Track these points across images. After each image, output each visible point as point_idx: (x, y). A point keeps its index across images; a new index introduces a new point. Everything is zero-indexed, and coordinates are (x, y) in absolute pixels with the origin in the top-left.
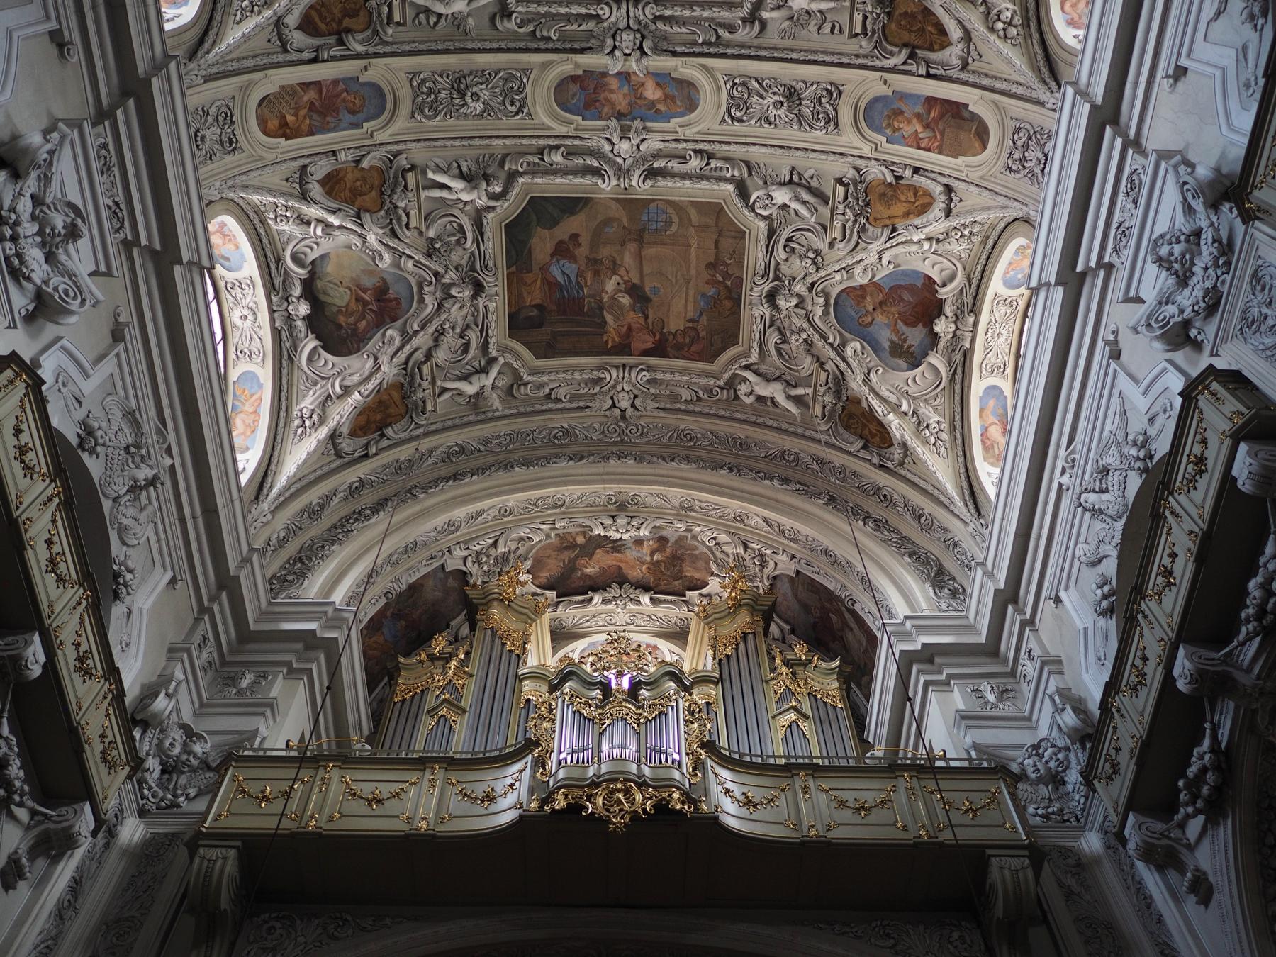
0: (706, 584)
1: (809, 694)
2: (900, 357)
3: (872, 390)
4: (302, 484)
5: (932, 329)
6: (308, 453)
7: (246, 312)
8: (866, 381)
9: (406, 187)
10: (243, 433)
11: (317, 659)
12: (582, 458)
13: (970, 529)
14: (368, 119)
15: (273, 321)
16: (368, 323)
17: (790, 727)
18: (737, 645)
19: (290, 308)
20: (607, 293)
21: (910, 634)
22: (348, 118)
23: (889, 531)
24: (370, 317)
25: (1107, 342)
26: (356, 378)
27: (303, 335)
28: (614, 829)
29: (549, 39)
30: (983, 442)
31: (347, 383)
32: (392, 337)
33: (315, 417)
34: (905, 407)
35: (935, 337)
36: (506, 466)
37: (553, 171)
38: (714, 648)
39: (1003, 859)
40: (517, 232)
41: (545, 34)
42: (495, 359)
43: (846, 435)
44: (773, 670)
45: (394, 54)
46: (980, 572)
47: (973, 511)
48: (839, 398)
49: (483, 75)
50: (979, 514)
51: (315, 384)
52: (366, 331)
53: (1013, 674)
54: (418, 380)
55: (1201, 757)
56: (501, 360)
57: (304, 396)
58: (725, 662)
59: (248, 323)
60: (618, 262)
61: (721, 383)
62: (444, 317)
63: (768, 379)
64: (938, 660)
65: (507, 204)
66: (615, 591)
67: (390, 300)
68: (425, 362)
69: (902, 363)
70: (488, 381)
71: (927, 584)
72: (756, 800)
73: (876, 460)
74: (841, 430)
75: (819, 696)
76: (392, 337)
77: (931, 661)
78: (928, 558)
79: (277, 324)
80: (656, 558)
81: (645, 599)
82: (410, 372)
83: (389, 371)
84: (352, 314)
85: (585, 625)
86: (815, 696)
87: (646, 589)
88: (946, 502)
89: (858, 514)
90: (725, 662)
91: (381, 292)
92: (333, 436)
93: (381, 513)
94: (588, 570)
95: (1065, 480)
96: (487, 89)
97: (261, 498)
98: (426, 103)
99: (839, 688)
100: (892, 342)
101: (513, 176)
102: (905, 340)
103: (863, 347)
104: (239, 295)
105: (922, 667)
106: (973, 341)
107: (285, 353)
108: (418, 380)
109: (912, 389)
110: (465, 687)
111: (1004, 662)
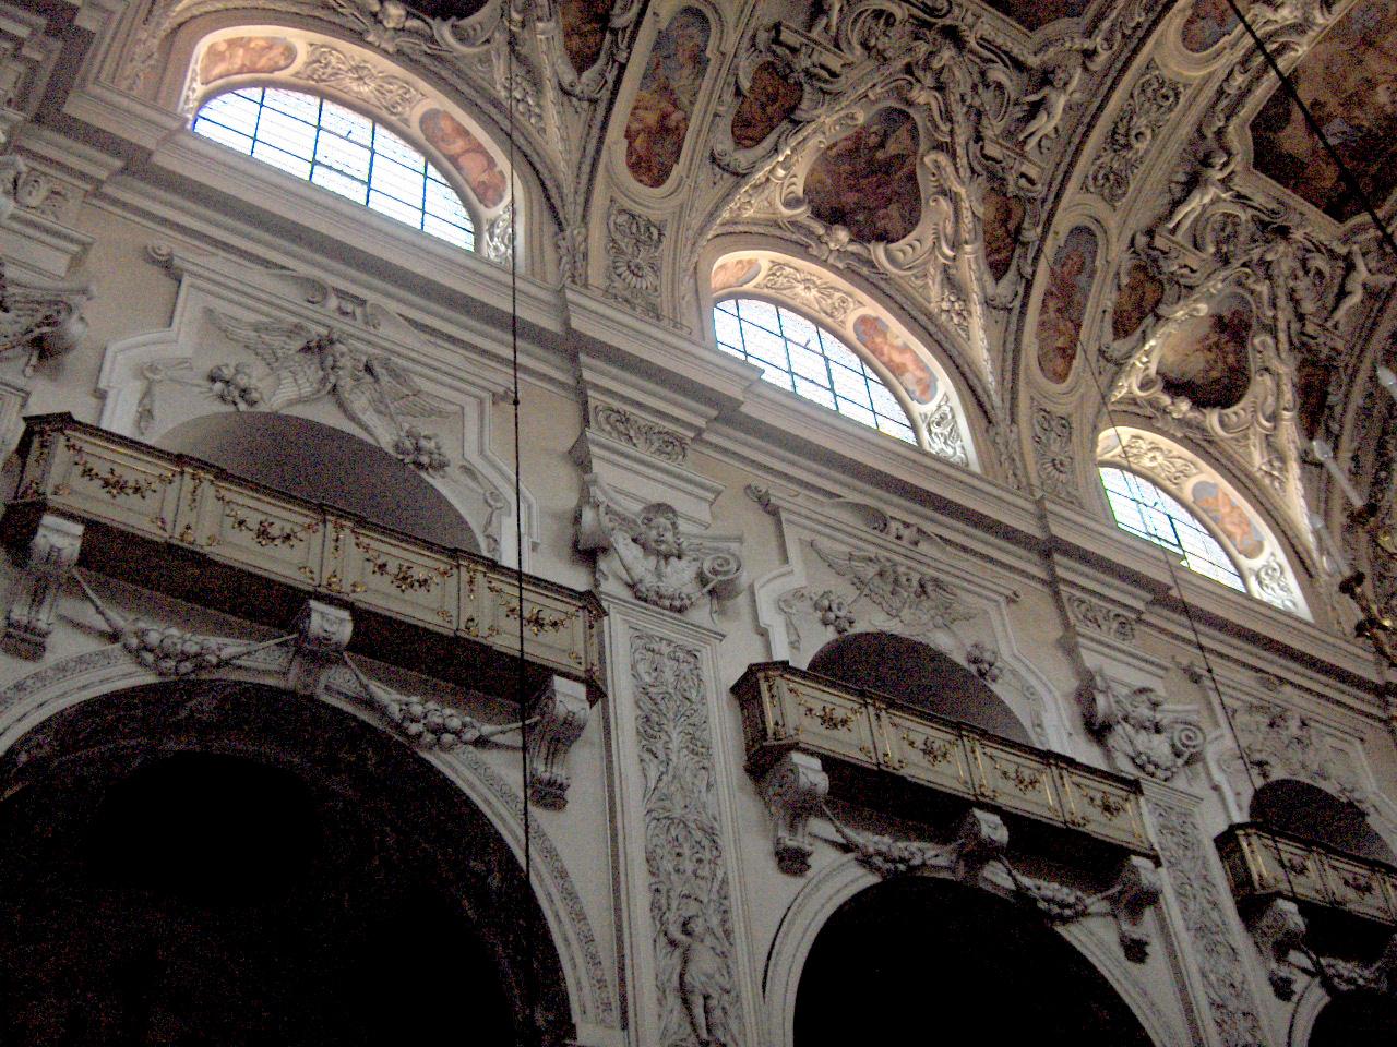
7: (1151, 454)
9: (1163, 252)
10: (1244, 533)
14: (1094, 254)
15: (1173, 437)
19: (1175, 415)
20: (1385, 105)
22: (1082, 279)
24: (1231, 347)
26: (1271, 400)
29: (1139, 25)
31: (1269, 411)
32: (1263, 343)
37: (1244, 94)
40: (1268, 160)
41: (1133, 24)
42: (1350, 253)
45: (1058, 197)
49: (1127, 116)
51: (1246, 437)
54: (1312, 342)
56: (1355, 248)
57: (1250, 454)
59: (1160, 459)
60: (1370, 77)
62: (1281, 281)
65: (1238, 158)
67: (1231, 320)
68: (1304, 325)
70: (1361, 273)
76: (1263, 343)
79: (1179, 435)
82: (1302, 346)
91: (1220, 323)
96: (1140, 117)
98: (1113, 184)
101: (1220, 133)
104: (1135, 451)
107: (1205, 444)
108: (1312, 342)
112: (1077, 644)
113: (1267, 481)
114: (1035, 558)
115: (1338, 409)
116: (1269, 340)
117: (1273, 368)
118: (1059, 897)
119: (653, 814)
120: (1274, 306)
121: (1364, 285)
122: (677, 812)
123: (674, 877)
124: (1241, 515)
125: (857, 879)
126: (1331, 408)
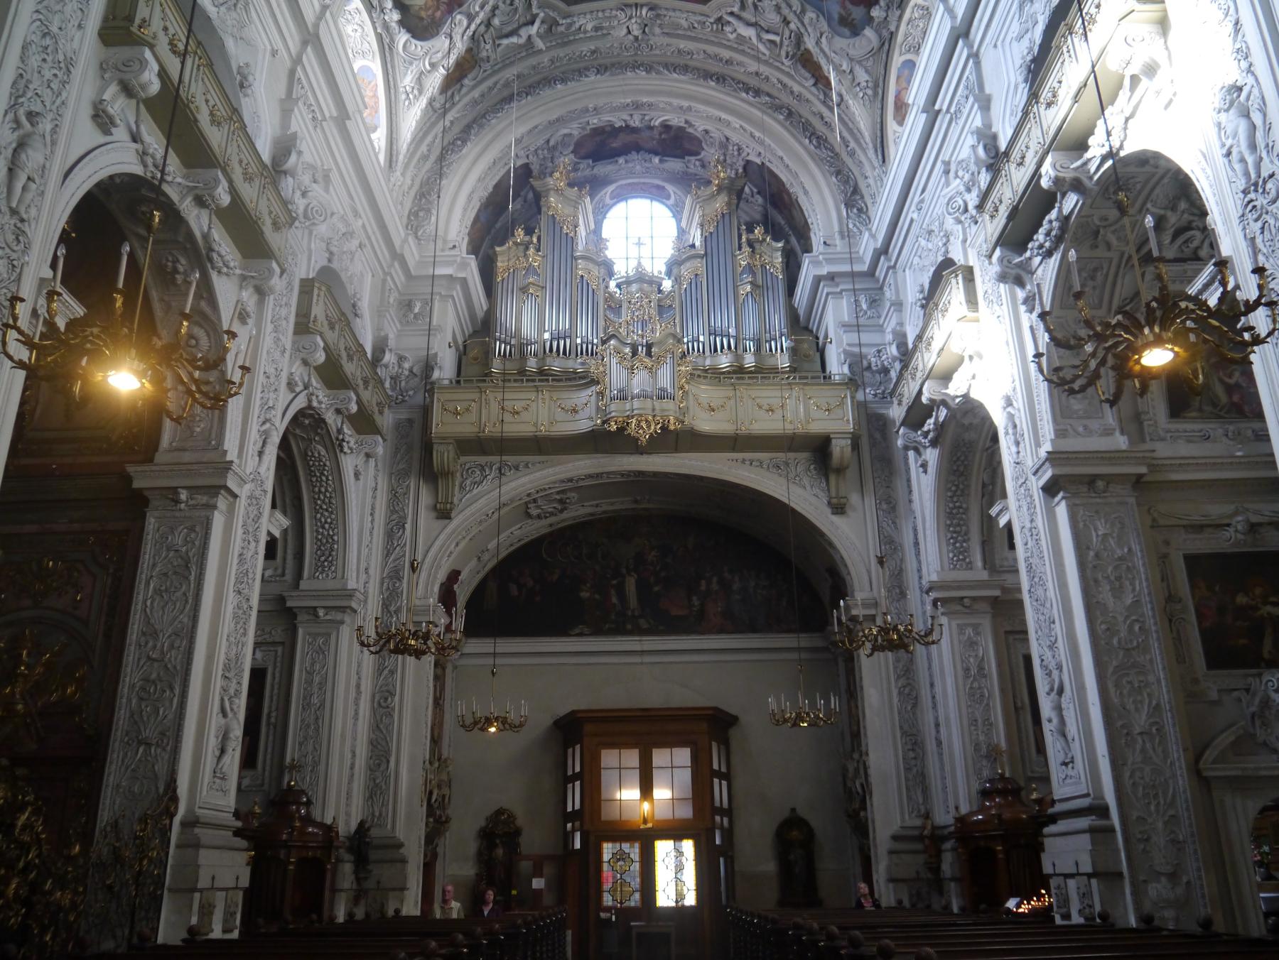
0: (699, 154)
1: (762, 266)
2: (845, 26)
3: (822, 50)
4: (418, 139)
5: (869, 12)
7: (356, 27)
8: (818, 43)
12: (606, 69)
13: (875, 174)
15: (375, 29)
16: (442, 12)
19: (386, 18)
21: (821, 262)
23: (826, 148)
24: (443, 7)
25: (943, 162)
26: (440, 55)
27: (397, 31)
30: (896, 104)
31: (434, 60)
32: (460, 20)
33: (416, 92)
34: (844, 67)
35: (871, 19)
36: (550, 82)
38: (702, 226)
42: (537, 14)
43: (802, 71)
44: (740, 248)
46: (867, 235)
47: (880, 157)
48: (799, 49)
50: (884, 161)
51: (411, 64)
52: (441, 19)
53: (881, 288)
55: (1050, 222)
57: (405, 74)
58: (709, 239)
59: (358, 34)
61: (712, 20)
63: (749, 24)
64: (837, 280)
66: (634, 155)
69: (846, 31)
70: (533, 30)
71: (843, 206)
73: (822, 97)
74: (800, 67)
79: (379, 31)
81: (656, 160)
83: (460, 46)
84: (429, 9)
87: (656, 154)
88: (864, 145)
89: (807, 130)
90: (709, 239)
92: (431, 102)
93: (469, 143)
94: (614, 145)
95: (915, 216)
97: (394, 165)
100: (841, 15)
102: (850, 14)
103: (818, 16)
104: (350, 17)
106: (898, 27)
107: (387, 47)
109: (852, 52)
111: (878, 281)
112: (293, 110)
113: (404, 97)
114: (297, 38)
115: (464, 90)
116: (465, 23)
117: (454, 39)
118: (228, 258)
119: (41, 17)
120: (482, 7)
121: (530, 37)
122: (54, 29)
123: (36, 74)
124: (377, 103)
125: (130, 163)
126: (462, 85)
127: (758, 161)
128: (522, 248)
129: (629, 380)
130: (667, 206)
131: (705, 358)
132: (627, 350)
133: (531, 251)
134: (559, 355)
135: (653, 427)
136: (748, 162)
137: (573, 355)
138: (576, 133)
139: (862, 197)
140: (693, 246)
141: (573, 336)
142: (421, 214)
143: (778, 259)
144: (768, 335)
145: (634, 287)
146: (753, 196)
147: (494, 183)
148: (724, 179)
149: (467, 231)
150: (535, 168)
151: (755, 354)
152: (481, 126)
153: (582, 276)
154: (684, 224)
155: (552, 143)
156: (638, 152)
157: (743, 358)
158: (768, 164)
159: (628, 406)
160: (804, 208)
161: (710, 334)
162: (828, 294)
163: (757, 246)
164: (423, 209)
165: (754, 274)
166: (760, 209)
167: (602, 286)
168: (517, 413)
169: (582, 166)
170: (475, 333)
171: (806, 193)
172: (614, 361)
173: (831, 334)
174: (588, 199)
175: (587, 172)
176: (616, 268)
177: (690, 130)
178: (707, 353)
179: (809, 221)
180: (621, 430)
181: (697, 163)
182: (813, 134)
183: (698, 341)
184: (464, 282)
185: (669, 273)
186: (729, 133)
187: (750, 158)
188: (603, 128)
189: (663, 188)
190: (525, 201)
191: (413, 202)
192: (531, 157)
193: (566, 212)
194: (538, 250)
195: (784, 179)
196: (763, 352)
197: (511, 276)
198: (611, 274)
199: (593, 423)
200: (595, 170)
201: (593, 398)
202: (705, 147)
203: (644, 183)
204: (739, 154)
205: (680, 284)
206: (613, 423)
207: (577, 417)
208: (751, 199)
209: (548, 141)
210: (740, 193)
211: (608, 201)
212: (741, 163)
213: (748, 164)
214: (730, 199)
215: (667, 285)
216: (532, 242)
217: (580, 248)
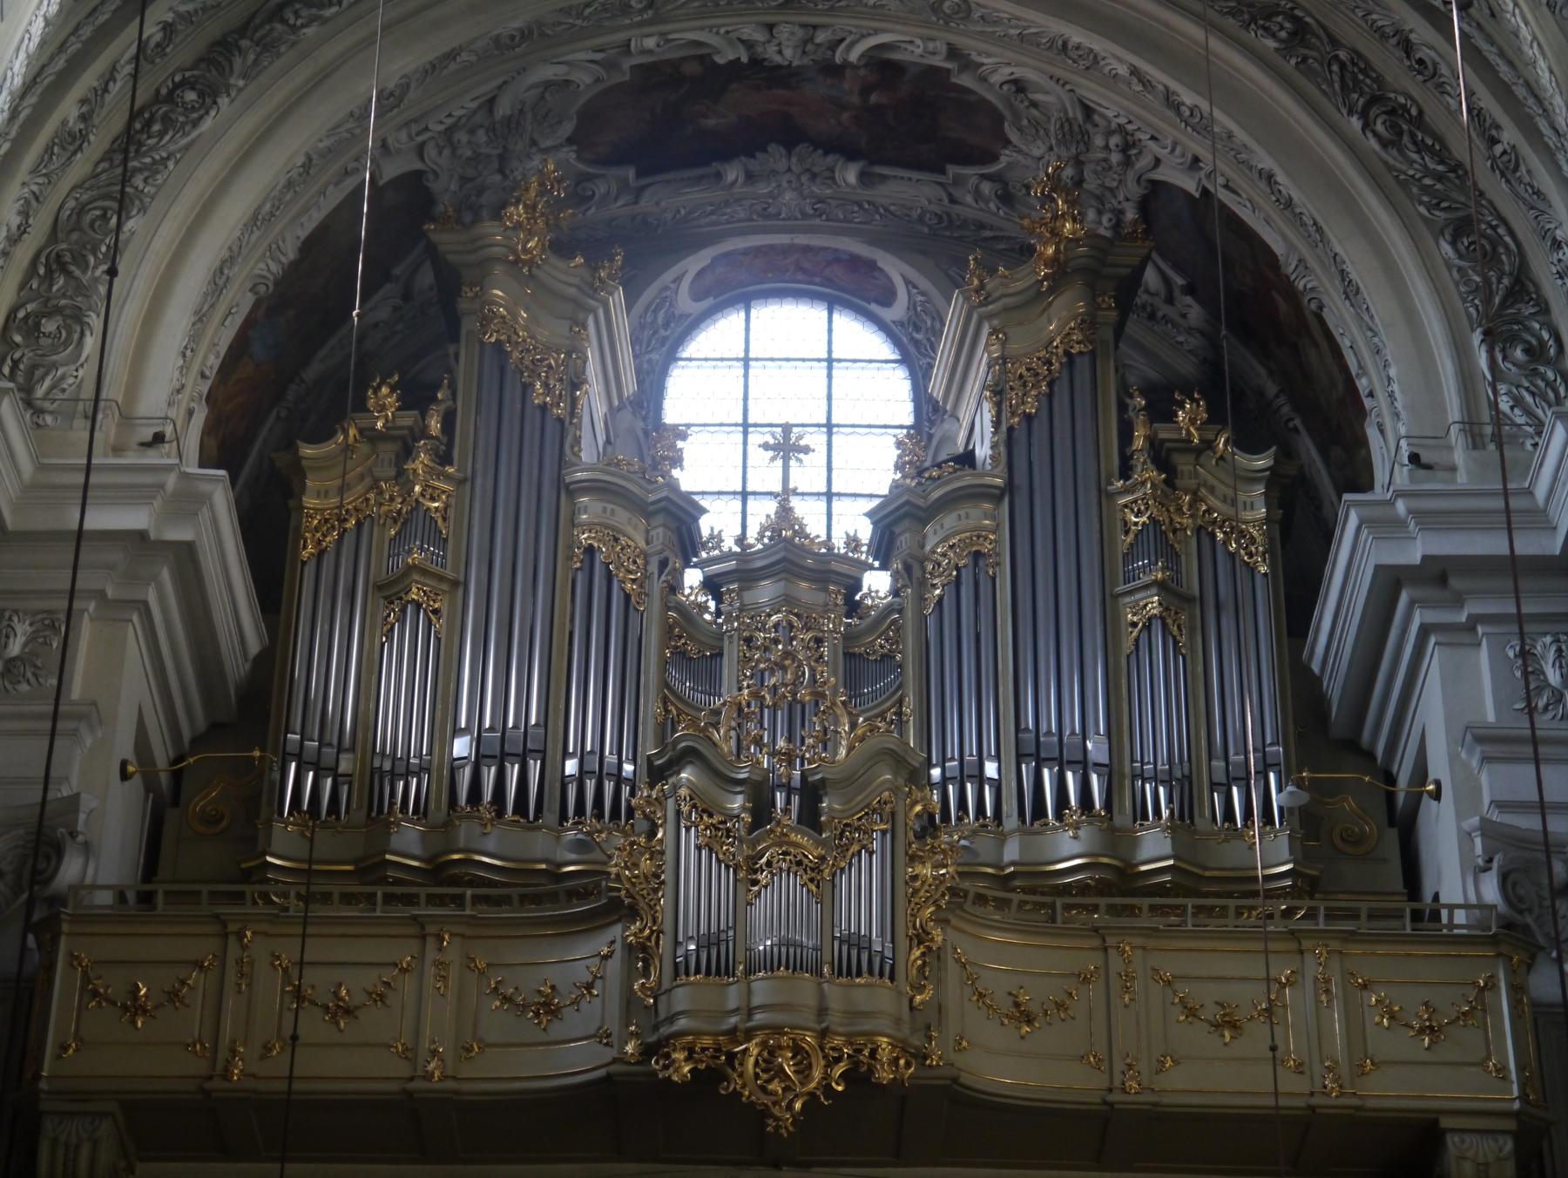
0: (995, 158)
1: (1199, 530)
6: (47, 22)
11: (155, 578)
17: (1148, 627)
18: (1050, 385)
21: (1401, 524)
23: (1420, 147)
28: (777, 1127)
38: (998, 392)
39: (1468, 1138)
44: (1125, 471)
58: (1021, 435)
64: (1455, 583)
66: (776, 156)
71: (1477, 337)
72: (1034, 1008)
75: (1220, 536)
77: (1442, 580)
78: (1496, 242)
80: (874, 98)
81: (850, 174)
85: (703, 221)
86: (1213, 535)
87: (851, 155)
90: (1021, 435)
93: (223, 101)
94: (711, 122)
99: (1268, 520)
105: (1419, 593)
110: (451, 513)
127: (1190, 185)
128: (388, 450)
129: (741, 906)
130: (882, 326)
131: (1002, 838)
132: (737, 803)
133: (422, 461)
134: (500, 812)
135: (817, 1074)
136: (1155, 184)
137: (550, 817)
138: (583, 78)
139: (1544, 310)
140: (967, 459)
141: (554, 750)
142: (49, 326)
143: (1256, 510)
144: (1218, 764)
145: (765, 592)
146: (1170, 300)
147: (303, 234)
148: (1076, 241)
149: (205, 387)
150: (445, 188)
151: (1173, 828)
152: (268, 47)
153: (590, 550)
154: (937, 387)
155: (504, 108)
156: (789, 146)
157: (1135, 843)
158: (1223, 195)
159: (733, 998)
160: (1345, 344)
161: (1020, 758)
162: (1425, 631)
163: (1183, 463)
164: (58, 310)
165: (1172, 557)
166: (1195, 342)
167: (657, 586)
168: (348, 1012)
169: (601, 188)
170: (215, 732)
171: (1351, 292)
172: (690, 840)
173: (1438, 767)
174: (618, 298)
175: (619, 208)
176: (706, 525)
177: (966, 80)
178: (1011, 821)
179: (1362, 384)
180: (708, 1079)
181: (986, 188)
182: (1374, 100)
183: (980, 779)
184: (186, 558)
185: (883, 549)
186: (1091, 91)
187: (1161, 175)
188: (674, 64)
189: (872, 266)
190: (407, 296)
191: (22, 286)
192: (431, 151)
193: (543, 335)
194: (445, 458)
195: (1278, 248)
196: (1201, 823)
197: (349, 540)
198: (687, 543)
199: (611, 1054)
200: (646, 204)
201: (615, 965)
202: (1013, 135)
203: (807, 249)
204: (1127, 163)
205: (923, 585)
206: (679, 1056)
207: (557, 1030)
208: (1164, 309)
209: (491, 103)
210: (1128, 287)
211: (685, 302)
212: (1134, 190)
213: (1155, 194)
214: (1094, 307)
215: (877, 583)
216: (424, 433)
217: (587, 455)
